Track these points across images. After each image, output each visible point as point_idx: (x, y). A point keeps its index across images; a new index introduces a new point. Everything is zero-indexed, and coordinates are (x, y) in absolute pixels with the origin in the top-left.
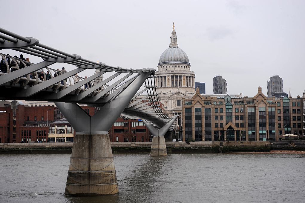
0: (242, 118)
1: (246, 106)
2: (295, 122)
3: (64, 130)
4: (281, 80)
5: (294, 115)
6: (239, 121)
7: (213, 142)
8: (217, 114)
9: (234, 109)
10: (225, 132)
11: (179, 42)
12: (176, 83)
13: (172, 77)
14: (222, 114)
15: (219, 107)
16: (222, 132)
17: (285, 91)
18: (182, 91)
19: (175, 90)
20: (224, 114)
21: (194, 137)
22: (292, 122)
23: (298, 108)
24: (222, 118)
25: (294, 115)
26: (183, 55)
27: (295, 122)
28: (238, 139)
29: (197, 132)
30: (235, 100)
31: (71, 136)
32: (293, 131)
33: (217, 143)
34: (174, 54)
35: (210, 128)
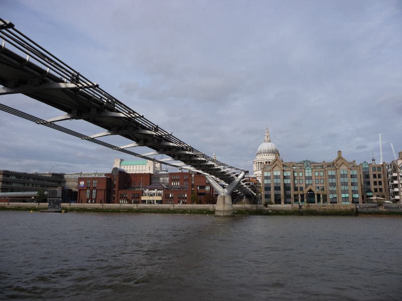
1: (326, 169)
2: (376, 187)
3: (154, 194)
5: (375, 180)
7: (292, 206)
9: (314, 173)
10: (305, 195)
16: (302, 196)
21: (273, 200)
23: (379, 173)
25: (375, 180)
27: (376, 187)
29: (276, 196)
30: (314, 165)
31: (160, 198)
32: (381, 196)
33: (296, 206)
35: (289, 192)
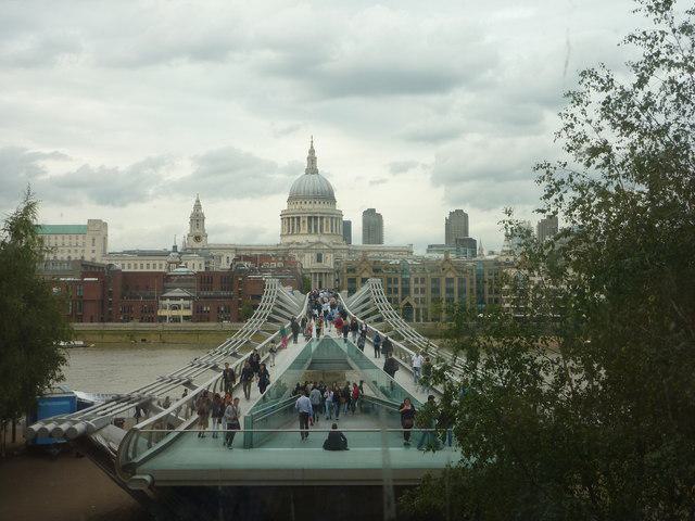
0: (423, 291)
4: (466, 216)
6: (420, 296)
8: (390, 286)
11: (320, 166)
12: (316, 227)
13: (310, 218)
14: (397, 286)
15: (393, 276)
17: (471, 235)
18: (324, 239)
19: (313, 239)
20: (399, 286)
22: (487, 296)
24: (396, 292)
26: (325, 185)
28: (418, 320)
31: (189, 313)
34: (311, 183)
